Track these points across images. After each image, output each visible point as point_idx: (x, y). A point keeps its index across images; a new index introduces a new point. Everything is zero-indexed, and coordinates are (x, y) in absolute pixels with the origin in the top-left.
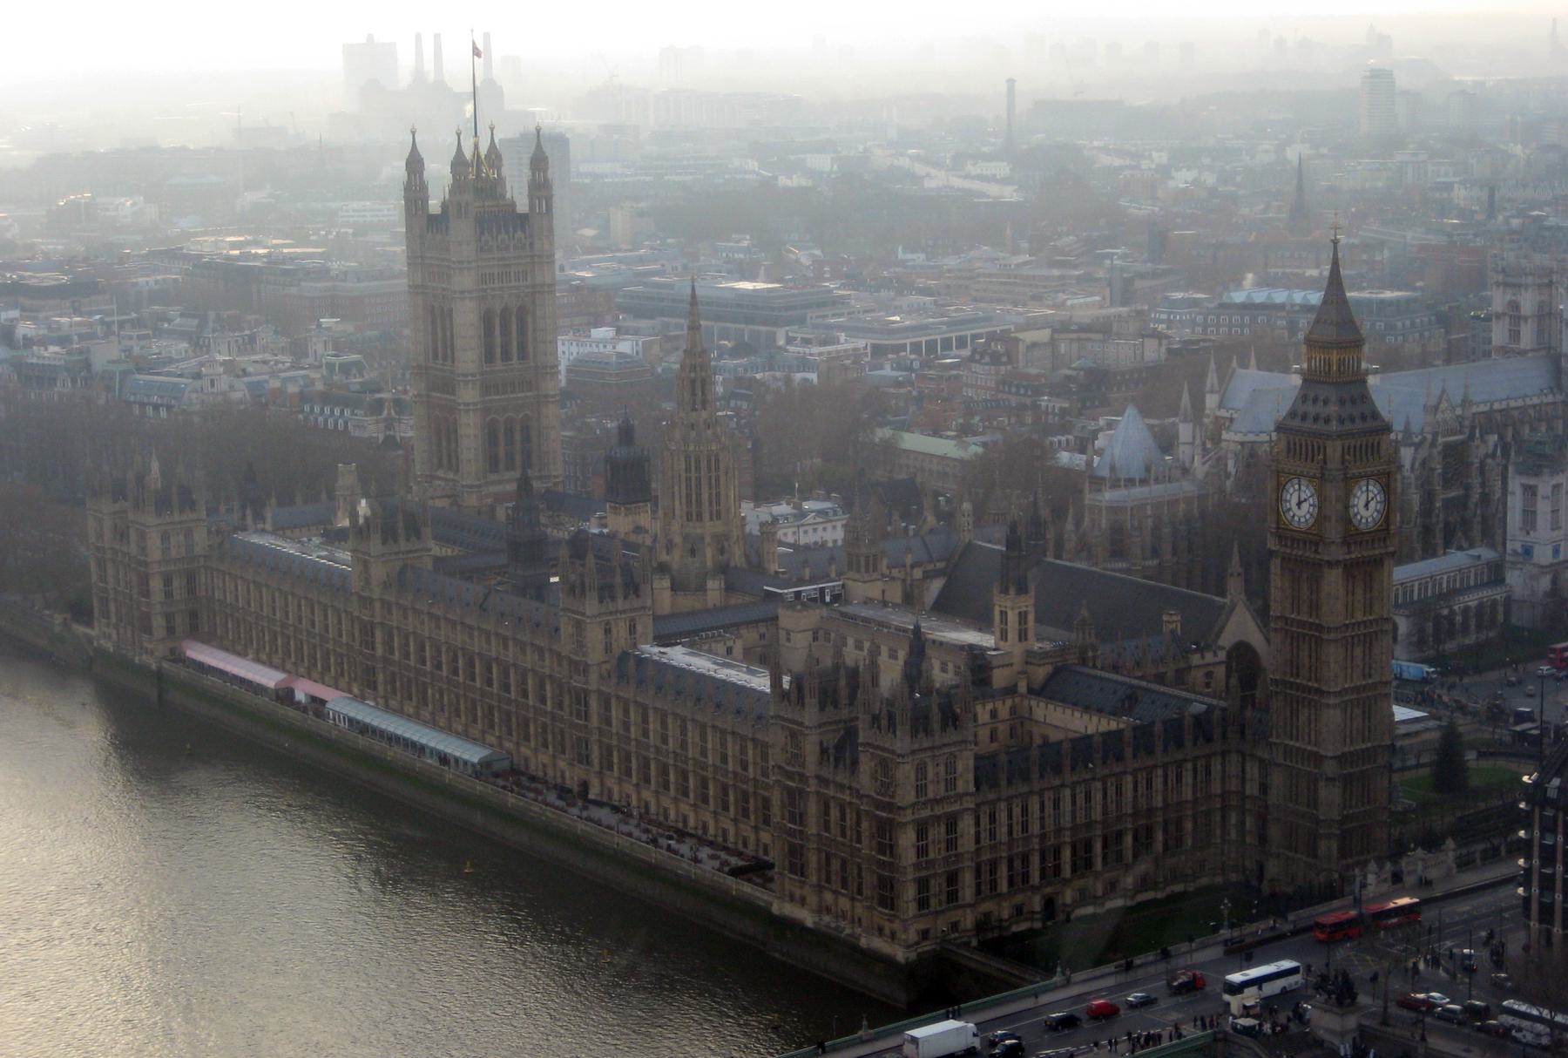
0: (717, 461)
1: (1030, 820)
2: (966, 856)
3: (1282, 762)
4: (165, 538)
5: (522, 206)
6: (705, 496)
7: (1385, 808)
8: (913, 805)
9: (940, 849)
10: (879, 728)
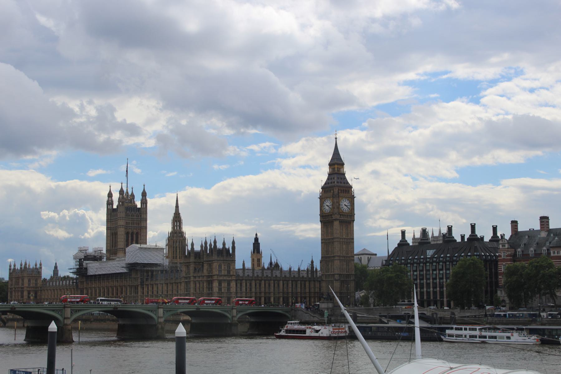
0: (182, 243)
1: (252, 288)
2: (233, 293)
3: (325, 280)
4: (29, 281)
5: (139, 206)
6: (178, 251)
7: (353, 292)
8: (218, 275)
9: (225, 289)
10: (209, 256)
